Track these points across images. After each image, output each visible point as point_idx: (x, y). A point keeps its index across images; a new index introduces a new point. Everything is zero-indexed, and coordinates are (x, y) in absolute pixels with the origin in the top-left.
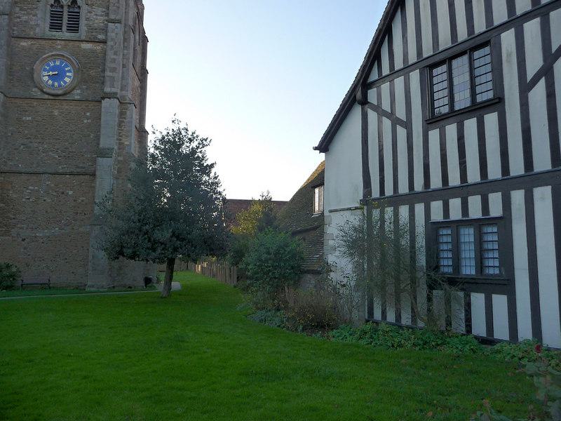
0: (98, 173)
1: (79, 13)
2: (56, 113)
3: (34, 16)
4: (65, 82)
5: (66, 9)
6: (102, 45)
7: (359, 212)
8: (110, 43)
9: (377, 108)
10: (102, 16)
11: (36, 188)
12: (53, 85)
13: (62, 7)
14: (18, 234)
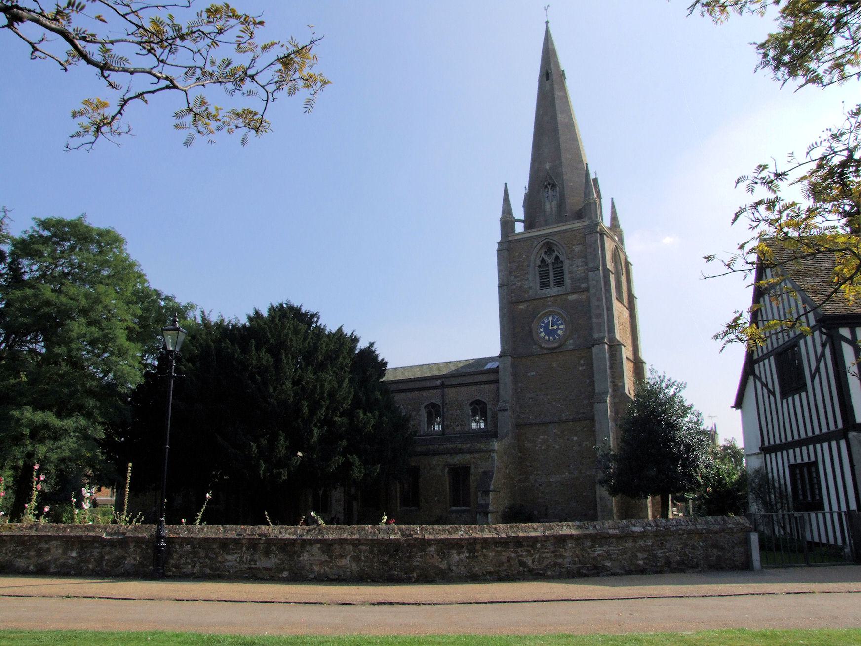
0: (596, 418)
1: (562, 267)
2: (554, 365)
3: (526, 280)
4: (559, 335)
5: (551, 267)
6: (585, 293)
7: (760, 456)
8: (592, 291)
9: (760, 379)
10: (582, 266)
11: (546, 437)
12: (549, 340)
13: (548, 265)
14: (536, 480)
